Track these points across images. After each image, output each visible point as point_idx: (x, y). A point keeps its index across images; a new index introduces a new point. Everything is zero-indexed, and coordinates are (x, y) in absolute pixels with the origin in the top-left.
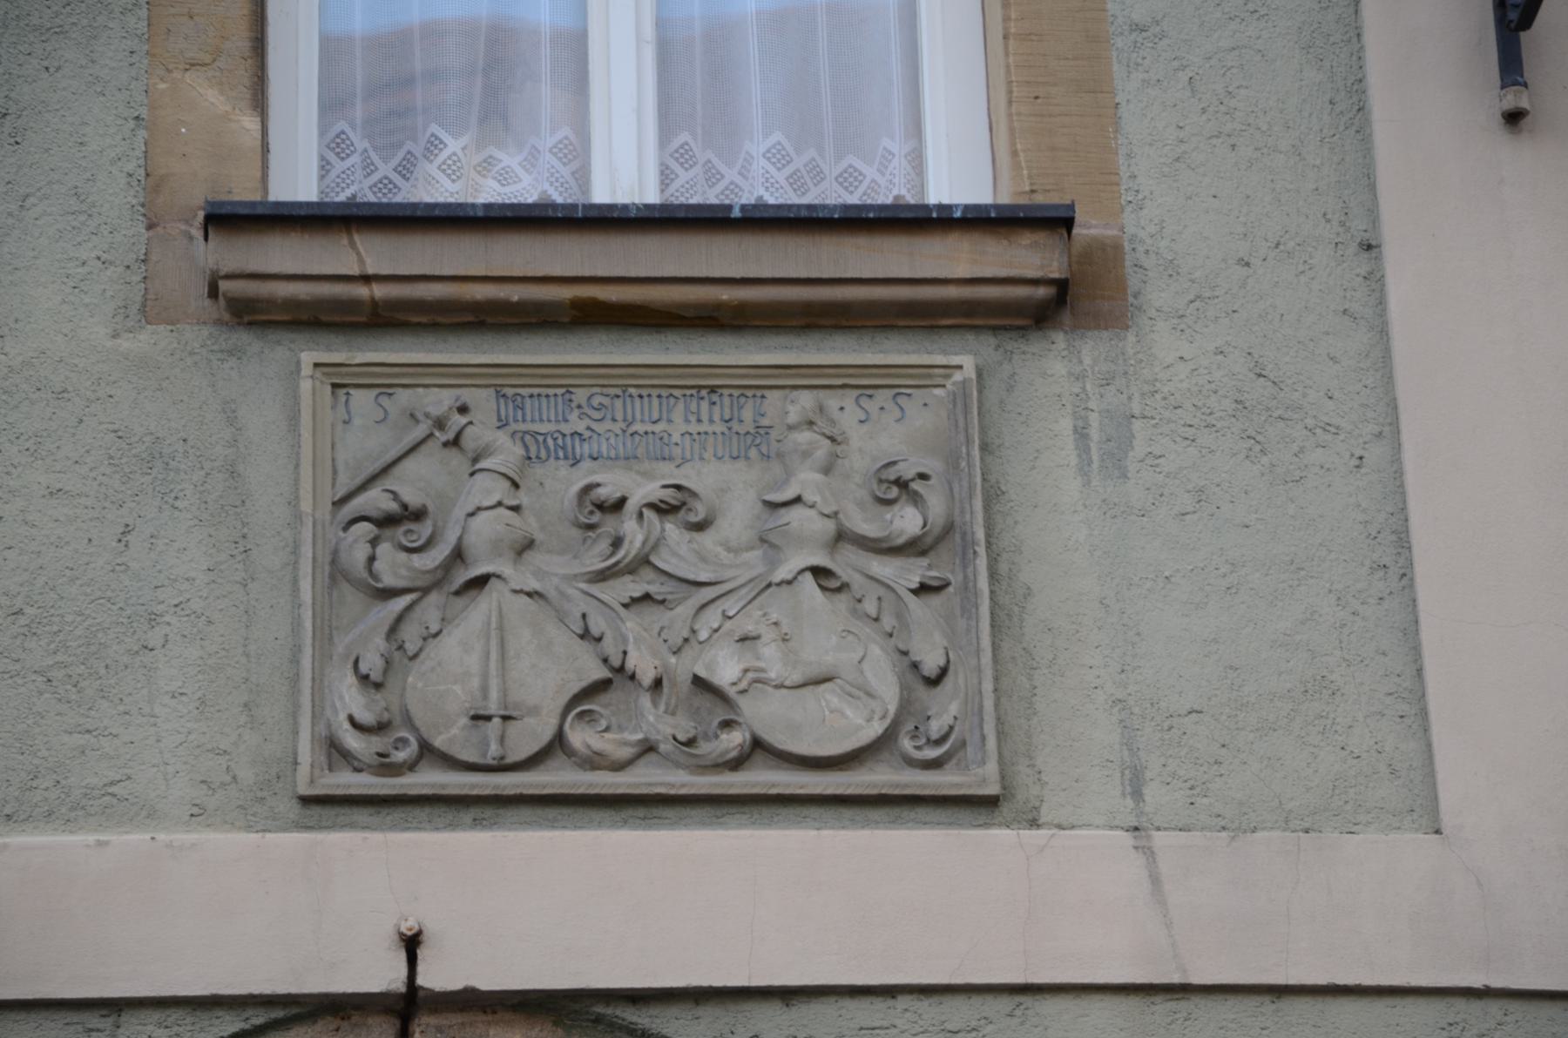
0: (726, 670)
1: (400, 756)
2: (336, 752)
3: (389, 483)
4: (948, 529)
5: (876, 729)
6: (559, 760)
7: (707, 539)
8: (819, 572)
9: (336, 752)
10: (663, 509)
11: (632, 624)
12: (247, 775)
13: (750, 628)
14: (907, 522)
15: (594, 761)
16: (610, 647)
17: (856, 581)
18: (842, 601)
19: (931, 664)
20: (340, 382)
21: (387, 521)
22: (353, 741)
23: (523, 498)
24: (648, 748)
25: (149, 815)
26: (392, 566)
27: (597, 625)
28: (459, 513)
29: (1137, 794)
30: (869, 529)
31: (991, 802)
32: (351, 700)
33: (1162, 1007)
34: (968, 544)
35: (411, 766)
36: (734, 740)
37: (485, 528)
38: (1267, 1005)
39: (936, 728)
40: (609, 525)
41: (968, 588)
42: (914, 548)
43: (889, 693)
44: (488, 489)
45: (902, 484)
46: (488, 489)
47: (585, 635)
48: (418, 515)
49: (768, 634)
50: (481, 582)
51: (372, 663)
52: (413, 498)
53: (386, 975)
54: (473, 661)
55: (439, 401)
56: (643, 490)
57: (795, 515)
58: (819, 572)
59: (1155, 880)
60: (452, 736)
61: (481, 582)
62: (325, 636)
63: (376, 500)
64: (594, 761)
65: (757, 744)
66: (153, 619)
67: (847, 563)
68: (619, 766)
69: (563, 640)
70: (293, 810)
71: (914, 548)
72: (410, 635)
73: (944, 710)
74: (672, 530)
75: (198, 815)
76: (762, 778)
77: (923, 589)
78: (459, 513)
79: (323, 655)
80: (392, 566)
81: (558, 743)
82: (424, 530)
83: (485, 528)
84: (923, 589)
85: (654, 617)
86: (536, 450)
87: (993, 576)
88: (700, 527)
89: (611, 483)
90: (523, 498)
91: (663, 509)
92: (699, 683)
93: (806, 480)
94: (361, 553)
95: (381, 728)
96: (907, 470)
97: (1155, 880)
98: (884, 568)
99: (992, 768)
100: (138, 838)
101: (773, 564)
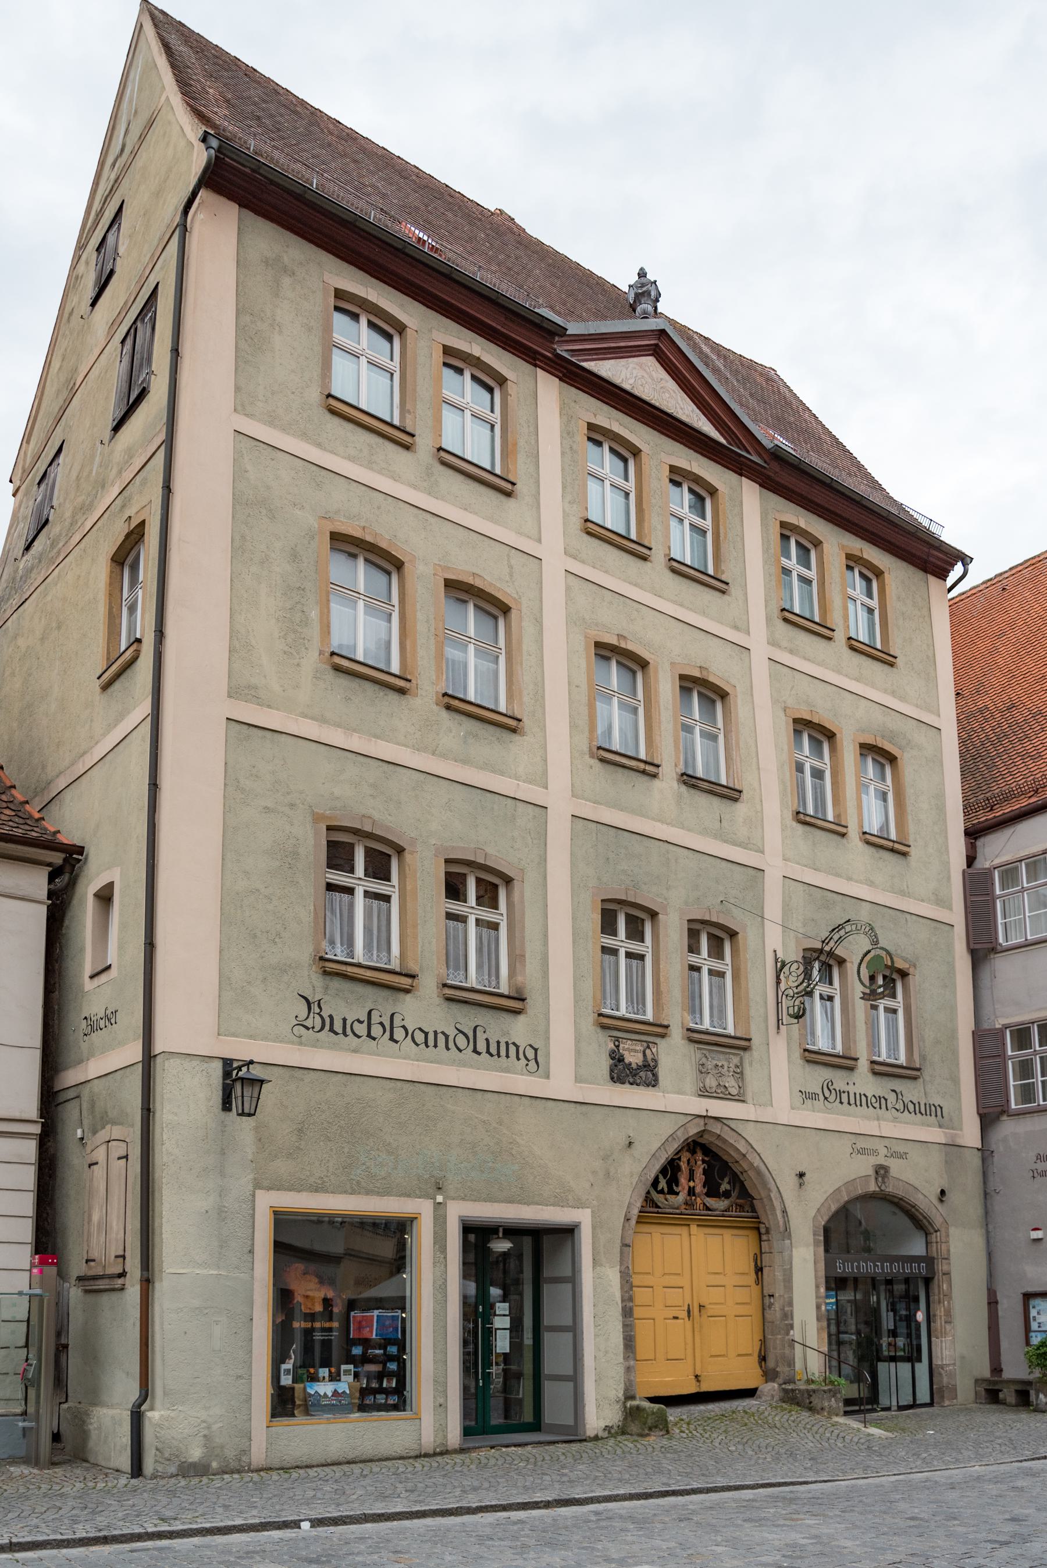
20: (698, 1048)
25: (687, 1095)
37: (710, 1067)
55: (705, 1052)
56: (720, 1064)
60: (708, 1089)
76: (729, 1097)
86: (713, 1059)
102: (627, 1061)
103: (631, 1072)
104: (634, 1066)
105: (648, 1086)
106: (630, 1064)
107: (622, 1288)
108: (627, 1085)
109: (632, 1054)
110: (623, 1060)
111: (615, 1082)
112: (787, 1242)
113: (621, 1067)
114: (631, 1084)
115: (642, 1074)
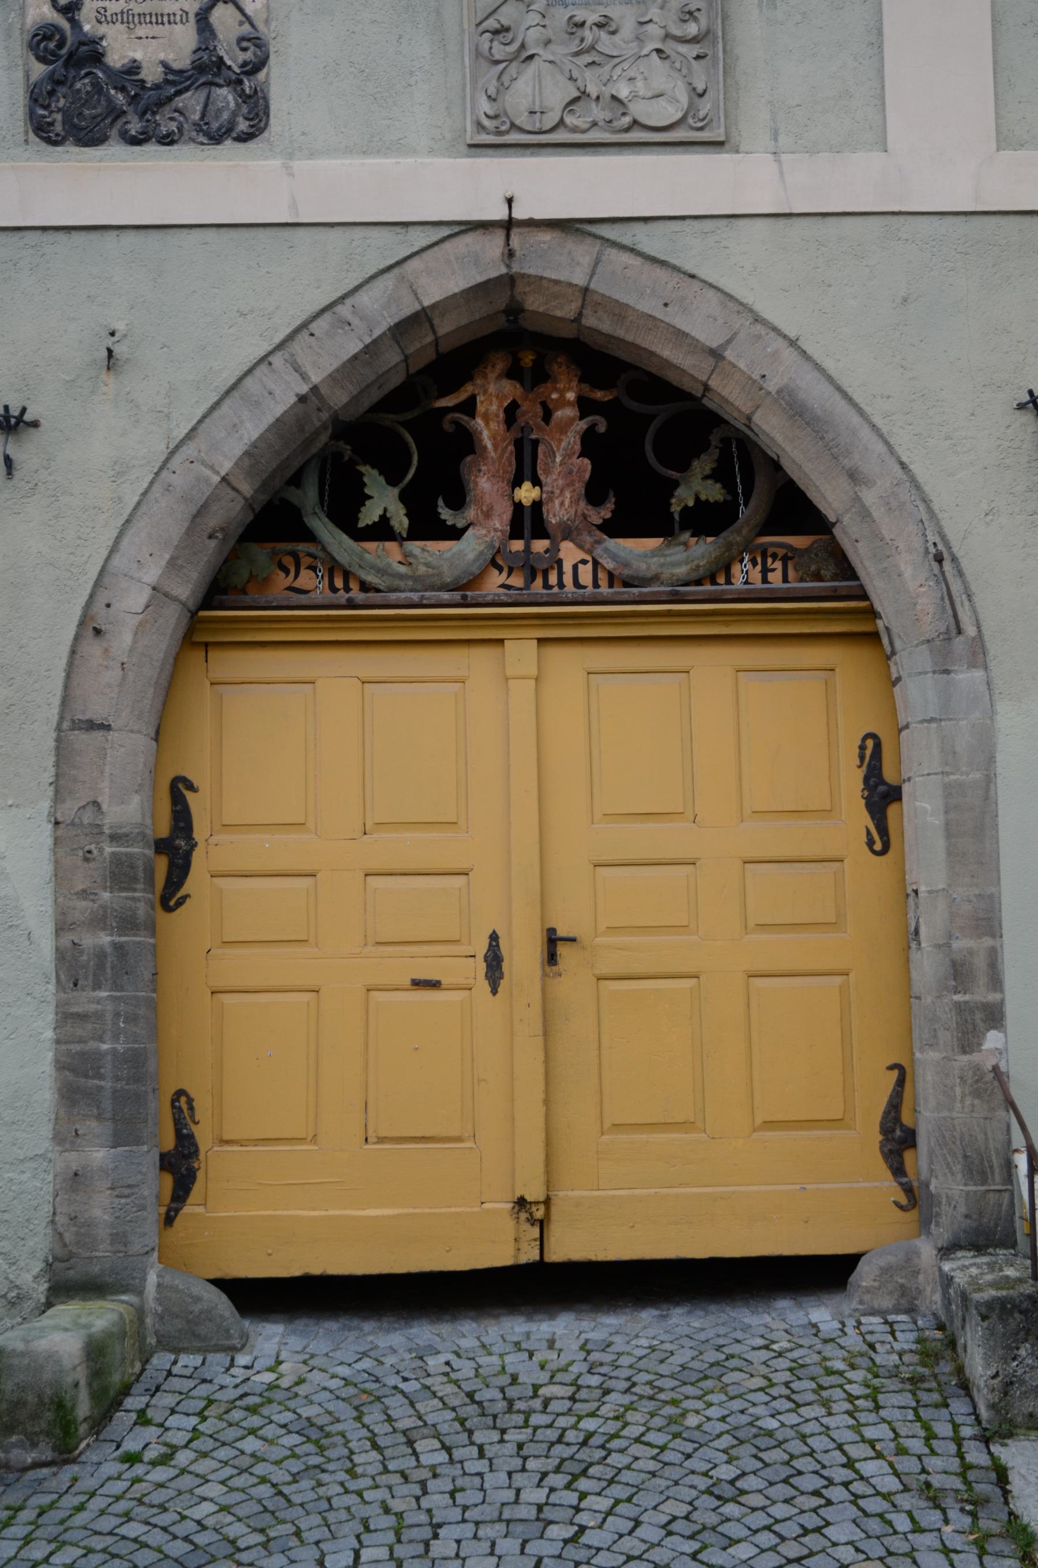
0: (623, 92)
1: (503, 128)
2: (480, 127)
3: (496, 16)
4: (708, 32)
5: (679, 115)
6: (561, 130)
7: (616, 38)
8: (659, 51)
9: (480, 127)
10: (600, 26)
11: (588, 74)
12: (448, 136)
13: (632, 74)
14: (692, 29)
15: (575, 130)
16: (580, 83)
17: (672, 54)
18: (667, 63)
19: (700, 88)
21: (496, 32)
22: (486, 122)
23: (546, 22)
24: (595, 124)
25: (413, 151)
26: (499, 51)
27: (576, 74)
28: (523, 28)
29: (776, 140)
30: (677, 32)
31: (721, 144)
32: (485, 106)
33: (782, 222)
34: (715, 38)
35: (507, 132)
36: (626, 120)
38: (819, 220)
39: (701, 114)
40: (580, 33)
41: (715, 57)
42: (695, 40)
43: (684, 99)
44: (534, 18)
45: (690, 13)
46: (534, 18)
47: (571, 78)
48: (507, 30)
49: (639, 77)
50: (531, 57)
51: (492, 91)
52: (505, 22)
53: (500, 213)
54: (529, 90)
56: (593, 18)
57: (650, 27)
58: (659, 51)
59: (781, 173)
60: (522, 120)
61: (531, 57)
62: (474, 80)
63: (492, 24)
64: (575, 130)
65: (635, 122)
66: (411, 73)
67: (669, 47)
68: (584, 132)
69: (563, 80)
70: (464, 149)
71: (695, 40)
72: (506, 79)
73: (705, 107)
74: (603, 34)
75: (431, 152)
77: (698, 57)
78: (523, 28)
79: (474, 88)
80: (499, 51)
81: (561, 122)
82: (510, 35)
83: (533, 34)
84: (698, 57)
85: (597, 70)
87: (725, 51)
88: (613, 33)
89: (580, 15)
90: (546, 22)
91: (600, 26)
92: (614, 98)
93: (654, 12)
94: (487, 46)
95: (496, 117)
96: (692, 7)
97: (781, 173)
98: (683, 49)
99: (722, 130)
100: (410, 160)
101: (641, 48)
102: (115, 59)
103: (134, 99)
104: (152, 74)
105: (216, 139)
106: (134, 68)
107: (60, 876)
108: (115, 150)
109: (142, 31)
110: (97, 57)
111: (49, 141)
112: (967, 678)
113: (83, 85)
114: (135, 141)
115: (192, 102)
